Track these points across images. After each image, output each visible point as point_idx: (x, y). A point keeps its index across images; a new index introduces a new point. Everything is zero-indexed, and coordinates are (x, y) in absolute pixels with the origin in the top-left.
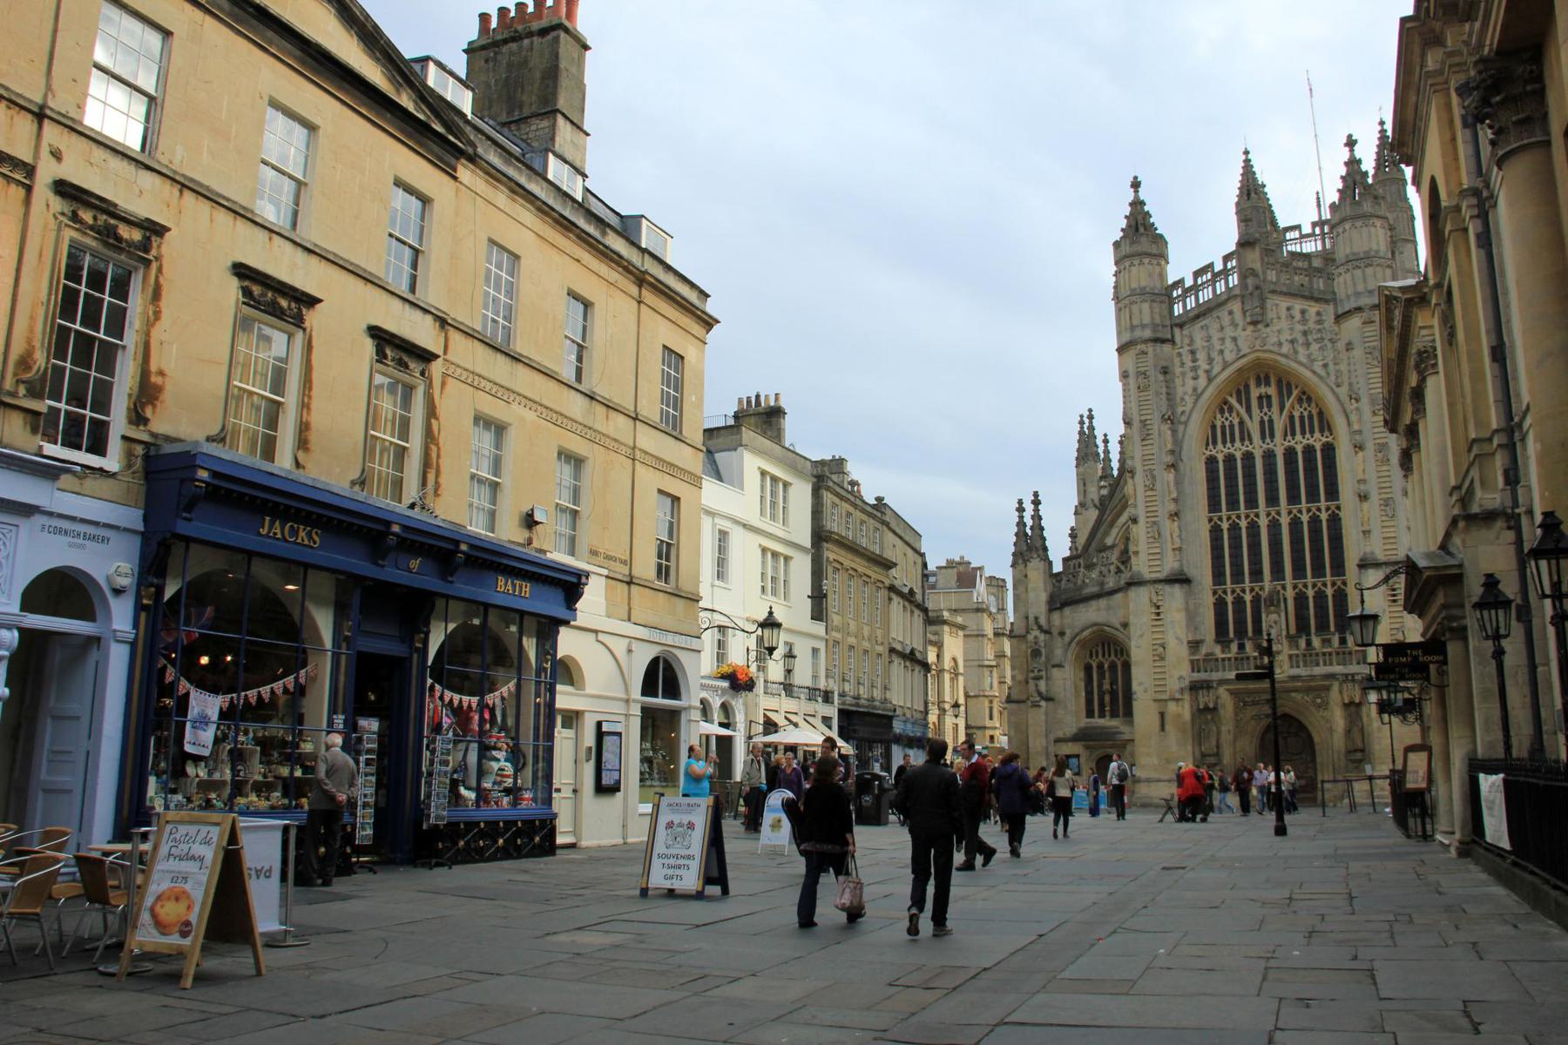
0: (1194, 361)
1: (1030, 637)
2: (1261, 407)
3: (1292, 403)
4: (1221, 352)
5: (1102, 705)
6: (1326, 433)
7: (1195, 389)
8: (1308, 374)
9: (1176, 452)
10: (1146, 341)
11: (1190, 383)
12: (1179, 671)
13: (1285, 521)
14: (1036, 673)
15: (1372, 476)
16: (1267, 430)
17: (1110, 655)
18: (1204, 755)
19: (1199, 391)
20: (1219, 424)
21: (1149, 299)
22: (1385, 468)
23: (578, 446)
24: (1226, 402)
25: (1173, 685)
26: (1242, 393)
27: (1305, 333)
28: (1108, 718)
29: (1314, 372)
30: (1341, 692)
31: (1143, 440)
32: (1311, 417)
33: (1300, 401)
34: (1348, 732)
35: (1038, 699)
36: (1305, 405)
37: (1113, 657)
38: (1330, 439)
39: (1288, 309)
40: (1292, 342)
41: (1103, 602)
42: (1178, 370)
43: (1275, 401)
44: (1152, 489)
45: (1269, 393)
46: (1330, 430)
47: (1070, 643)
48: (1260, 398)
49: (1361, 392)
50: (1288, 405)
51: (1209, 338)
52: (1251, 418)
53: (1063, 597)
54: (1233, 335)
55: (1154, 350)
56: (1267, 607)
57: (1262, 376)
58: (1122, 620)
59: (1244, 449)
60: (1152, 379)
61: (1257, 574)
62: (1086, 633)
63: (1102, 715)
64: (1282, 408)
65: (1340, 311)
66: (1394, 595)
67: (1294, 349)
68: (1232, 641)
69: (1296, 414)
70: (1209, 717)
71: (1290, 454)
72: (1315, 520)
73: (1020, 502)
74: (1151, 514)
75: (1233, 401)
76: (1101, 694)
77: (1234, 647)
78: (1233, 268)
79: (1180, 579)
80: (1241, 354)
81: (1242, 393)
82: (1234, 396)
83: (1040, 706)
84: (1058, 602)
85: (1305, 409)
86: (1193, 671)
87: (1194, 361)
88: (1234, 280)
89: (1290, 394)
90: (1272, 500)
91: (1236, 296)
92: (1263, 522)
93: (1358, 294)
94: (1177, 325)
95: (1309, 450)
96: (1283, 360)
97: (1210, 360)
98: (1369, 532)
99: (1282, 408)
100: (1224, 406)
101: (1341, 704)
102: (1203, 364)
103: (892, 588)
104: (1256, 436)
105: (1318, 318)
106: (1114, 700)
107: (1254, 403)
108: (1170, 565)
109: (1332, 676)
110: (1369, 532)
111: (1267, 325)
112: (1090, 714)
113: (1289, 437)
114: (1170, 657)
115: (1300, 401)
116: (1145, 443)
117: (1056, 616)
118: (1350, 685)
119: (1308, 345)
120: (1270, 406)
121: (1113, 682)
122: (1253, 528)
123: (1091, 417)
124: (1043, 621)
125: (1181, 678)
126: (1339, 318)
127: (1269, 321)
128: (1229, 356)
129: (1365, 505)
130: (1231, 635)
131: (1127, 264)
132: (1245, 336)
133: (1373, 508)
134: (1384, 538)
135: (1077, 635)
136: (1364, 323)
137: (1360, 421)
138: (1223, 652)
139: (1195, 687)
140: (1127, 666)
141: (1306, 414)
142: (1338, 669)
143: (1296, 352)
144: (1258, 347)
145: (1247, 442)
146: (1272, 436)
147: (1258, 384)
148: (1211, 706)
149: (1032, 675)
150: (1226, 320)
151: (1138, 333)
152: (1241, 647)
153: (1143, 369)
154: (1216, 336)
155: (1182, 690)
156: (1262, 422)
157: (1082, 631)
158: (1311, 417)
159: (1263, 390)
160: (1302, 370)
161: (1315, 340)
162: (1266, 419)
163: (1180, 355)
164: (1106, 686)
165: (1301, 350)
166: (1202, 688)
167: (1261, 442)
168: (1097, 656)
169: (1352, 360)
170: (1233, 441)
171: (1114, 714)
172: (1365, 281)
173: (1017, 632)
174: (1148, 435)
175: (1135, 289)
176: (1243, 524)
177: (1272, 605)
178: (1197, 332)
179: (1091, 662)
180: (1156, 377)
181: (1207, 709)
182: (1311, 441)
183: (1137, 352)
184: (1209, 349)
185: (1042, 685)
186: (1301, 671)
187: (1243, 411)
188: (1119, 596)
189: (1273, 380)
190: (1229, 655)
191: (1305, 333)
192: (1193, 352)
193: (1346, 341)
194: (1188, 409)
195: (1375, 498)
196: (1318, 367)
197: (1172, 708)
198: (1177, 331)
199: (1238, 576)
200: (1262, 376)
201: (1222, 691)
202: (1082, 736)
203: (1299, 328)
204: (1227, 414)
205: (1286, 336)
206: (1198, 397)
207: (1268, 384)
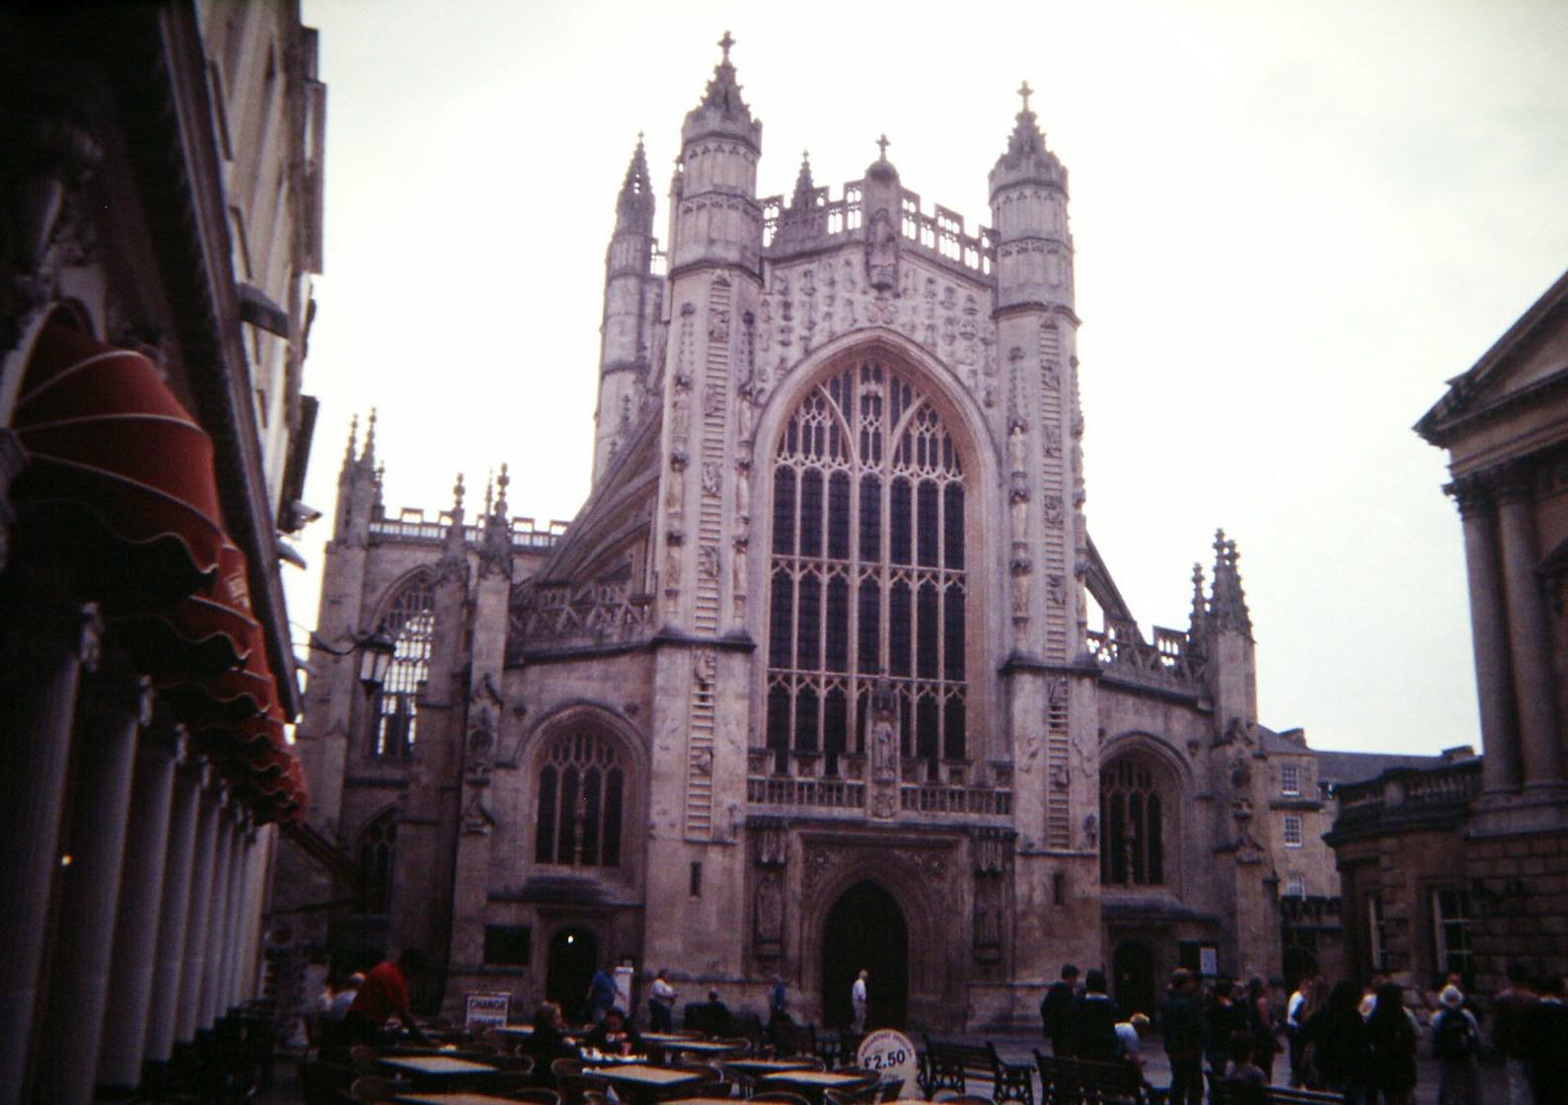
0: (787, 318)
1: (474, 709)
2: (865, 412)
3: (912, 417)
4: (828, 316)
6: (953, 470)
7: (783, 360)
10: (730, 266)
11: (778, 350)
12: (731, 801)
13: (886, 584)
16: (872, 447)
17: (588, 758)
19: (790, 364)
20: (802, 423)
21: (741, 207)
22: (1055, 532)
24: (815, 392)
25: (720, 820)
28: (577, 864)
30: (972, 853)
31: (708, 415)
32: (933, 441)
36: (927, 424)
37: (593, 761)
38: (959, 479)
39: (931, 281)
40: (931, 327)
41: (596, 668)
44: (714, 496)
45: (881, 394)
46: (958, 466)
47: (534, 727)
48: (866, 399)
49: (1028, 419)
50: (905, 417)
51: (811, 292)
52: (848, 421)
53: (528, 648)
54: (847, 295)
55: (740, 284)
56: (877, 709)
57: (871, 367)
59: (835, 467)
60: (733, 324)
62: (565, 714)
63: (566, 859)
65: (1003, 302)
66: (1054, 717)
67: (933, 338)
69: (915, 434)
70: (772, 876)
71: (901, 488)
72: (927, 592)
74: (708, 534)
75: (827, 393)
76: (569, 820)
77: (820, 768)
78: (854, 203)
79: (741, 645)
80: (858, 326)
82: (829, 385)
83: (481, 834)
84: (517, 659)
85: (927, 430)
86: (750, 798)
87: (787, 318)
88: (856, 220)
89: (907, 404)
90: (870, 550)
91: (858, 243)
92: (855, 581)
94: (768, 259)
95: (928, 489)
96: (914, 350)
97: (811, 326)
98: (1025, 620)
100: (811, 398)
101: (969, 871)
102: (799, 330)
105: (969, 305)
106: (589, 838)
107: (857, 404)
108: (729, 623)
109: (963, 829)
110: (1025, 620)
111: (897, 296)
112: (543, 854)
113: (901, 465)
114: (719, 772)
115: (920, 415)
116: (710, 420)
117: (514, 678)
118: (991, 845)
119: (952, 338)
120: (878, 413)
121: (593, 805)
122: (839, 587)
123: (373, 419)
124: (497, 681)
125: (732, 810)
126: (997, 314)
127: (900, 290)
128: (839, 326)
129: (1024, 580)
131: (712, 145)
132: (865, 302)
134: (1050, 633)
136: (1043, 326)
137: (1025, 460)
138: (801, 773)
139: (756, 829)
140: (616, 780)
141: (928, 436)
142: (973, 817)
143: (934, 345)
144: (881, 323)
145: (840, 459)
146: (877, 458)
149: (470, 776)
150: (840, 275)
151: (719, 252)
153: (721, 308)
154: (823, 290)
155: (735, 828)
156: (865, 434)
158: (933, 441)
159: (873, 386)
161: (962, 334)
162: (871, 430)
163: (765, 304)
164: (581, 810)
165: (940, 342)
166: (769, 828)
167: (860, 462)
168: (566, 758)
169: (1019, 374)
170: (819, 452)
171: (588, 861)
172: (1045, 270)
173: (432, 700)
174: (717, 409)
175: (720, 187)
176: (825, 579)
177: (885, 707)
178: (795, 275)
179: (555, 764)
180: (736, 324)
182: (933, 476)
183: (714, 278)
184: (811, 307)
186: (912, 816)
187: (839, 411)
188: (624, 662)
189: (888, 376)
190: (811, 779)
191: (950, 321)
192: (787, 305)
193: (1010, 346)
194: (769, 387)
196: (963, 372)
197: (715, 859)
198: (767, 268)
200: (871, 367)
202: (537, 894)
203: (941, 313)
204: (814, 411)
206: (790, 371)
207: (879, 379)
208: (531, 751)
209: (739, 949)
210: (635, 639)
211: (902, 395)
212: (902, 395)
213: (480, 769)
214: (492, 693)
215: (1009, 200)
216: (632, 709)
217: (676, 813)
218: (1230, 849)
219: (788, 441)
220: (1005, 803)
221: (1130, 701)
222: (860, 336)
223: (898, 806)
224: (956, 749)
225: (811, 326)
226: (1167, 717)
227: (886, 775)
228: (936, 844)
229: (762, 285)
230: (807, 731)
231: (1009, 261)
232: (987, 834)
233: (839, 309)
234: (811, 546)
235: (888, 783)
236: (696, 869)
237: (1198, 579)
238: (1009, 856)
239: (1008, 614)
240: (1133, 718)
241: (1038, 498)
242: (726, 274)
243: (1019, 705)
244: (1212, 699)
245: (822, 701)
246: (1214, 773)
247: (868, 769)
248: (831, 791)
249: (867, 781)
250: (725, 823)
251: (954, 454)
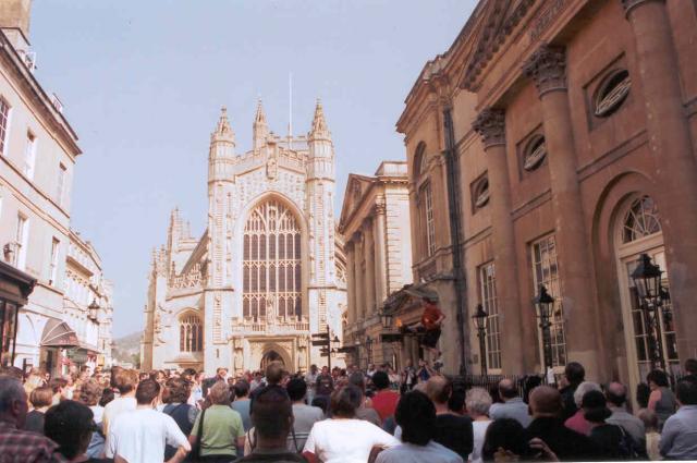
1: (156, 313)
5: (188, 345)
16: (273, 225)
23: (26, 211)
25: (223, 337)
33: (287, 214)
42: (233, 195)
61: (263, 288)
71: (282, 236)
73: (154, 249)
75: (258, 211)
76: (188, 340)
90: (272, 256)
92: (268, 266)
95: (290, 236)
103: (91, 286)
104: (267, 227)
112: (182, 349)
122: (263, 268)
139: (234, 339)
140: (201, 328)
152: (256, 320)
159: (273, 208)
181: (239, 349)
187: (262, 216)
197: (221, 347)
199: (255, 289)
205: (284, 186)
207: (274, 205)
225: (249, 193)
230: (255, 309)
236: (218, 351)
242: (221, 183)
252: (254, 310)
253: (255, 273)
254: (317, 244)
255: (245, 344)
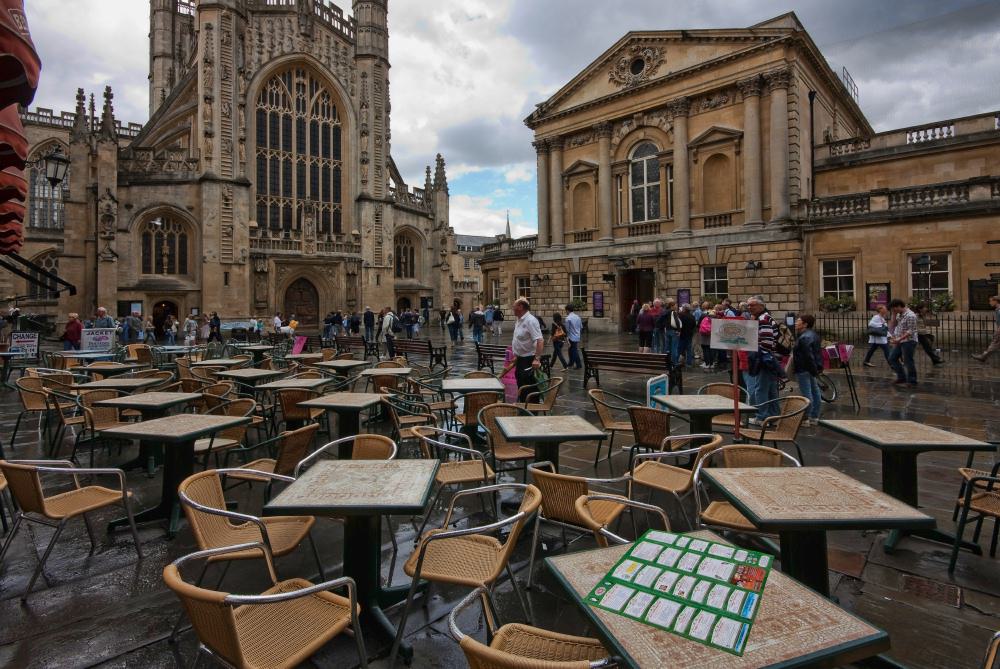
0: (261, 41)
1: (103, 205)
2: (298, 90)
4: (281, 44)
7: (260, 60)
8: (335, 81)
9: (247, 92)
11: (256, 55)
12: (242, 247)
14: (107, 235)
15: (371, 149)
16: (301, 105)
18: (257, 302)
25: (237, 255)
26: (287, 77)
27: (337, 56)
29: (339, 82)
30: (346, 268)
33: (323, 95)
34: (348, 290)
35: (110, 256)
40: (329, 58)
41: (170, 189)
43: (308, 89)
47: (137, 214)
48: (298, 84)
50: (316, 95)
56: (306, 213)
58: (188, 204)
64: (311, 98)
65: (358, 53)
68: (281, 230)
77: (282, 235)
79: (244, 183)
80: (295, 51)
81: (287, 77)
84: (126, 180)
87: (261, 41)
90: (301, 149)
93: (373, 47)
96: (321, 67)
97: (273, 46)
99: (311, 98)
100: (272, 79)
104: (294, 107)
109: (342, 258)
111: (313, 41)
113: (314, 115)
114: (236, 235)
115: (323, 95)
117: (124, 192)
120: (304, 92)
122: (287, 163)
124: (114, 192)
125: (242, 251)
126: (357, 57)
128: (286, 50)
129: (366, 166)
130: (281, 226)
133: (370, 168)
135: (144, 209)
138: (274, 236)
139: (255, 258)
142: (345, 254)
143: (330, 65)
146: (304, 111)
147: (298, 76)
148: (266, 270)
149: (103, 235)
150: (286, 25)
156: (298, 100)
157: (150, 207)
159: (301, 79)
160: (332, 77)
165: (332, 65)
170: (277, 104)
185: (113, 245)
189: (308, 76)
194: (253, 71)
195: (372, 162)
196: (342, 79)
197: (235, 270)
201: (271, 261)
204: (274, 86)
207: (304, 76)
208: (136, 224)
209: (247, 305)
210: (190, 177)
211: (314, 86)
212: (314, 86)
213: (108, 233)
214: (112, 198)
215: (362, 8)
216: (191, 208)
217: (216, 252)
218: (438, 266)
219: (263, 96)
220: (359, 249)
221: (404, 214)
222: (297, 56)
223: (315, 250)
224: (337, 230)
225: (273, 46)
226: (418, 220)
227: (310, 238)
228: (332, 264)
229: (247, 22)
230: (275, 220)
231: (361, 34)
232: (351, 260)
233: (286, 42)
234: (275, 145)
235: (311, 241)
236: (226, 275)
237: (428, 172)
238: (360, 268)
239: (359, 179)
240: (406, 220)
241: (372, 134)
243: (363, 214)
244: (434, 215)
245: (281, 209)
246: (433, 240)
247: (302, 236)
248: (287, 243)
249: (302, 240)
250: (240, 256)
251: (336, 112)
252: (272, 221)
253: (275, 172)
254: (371, 146)
255: (270, 265)
